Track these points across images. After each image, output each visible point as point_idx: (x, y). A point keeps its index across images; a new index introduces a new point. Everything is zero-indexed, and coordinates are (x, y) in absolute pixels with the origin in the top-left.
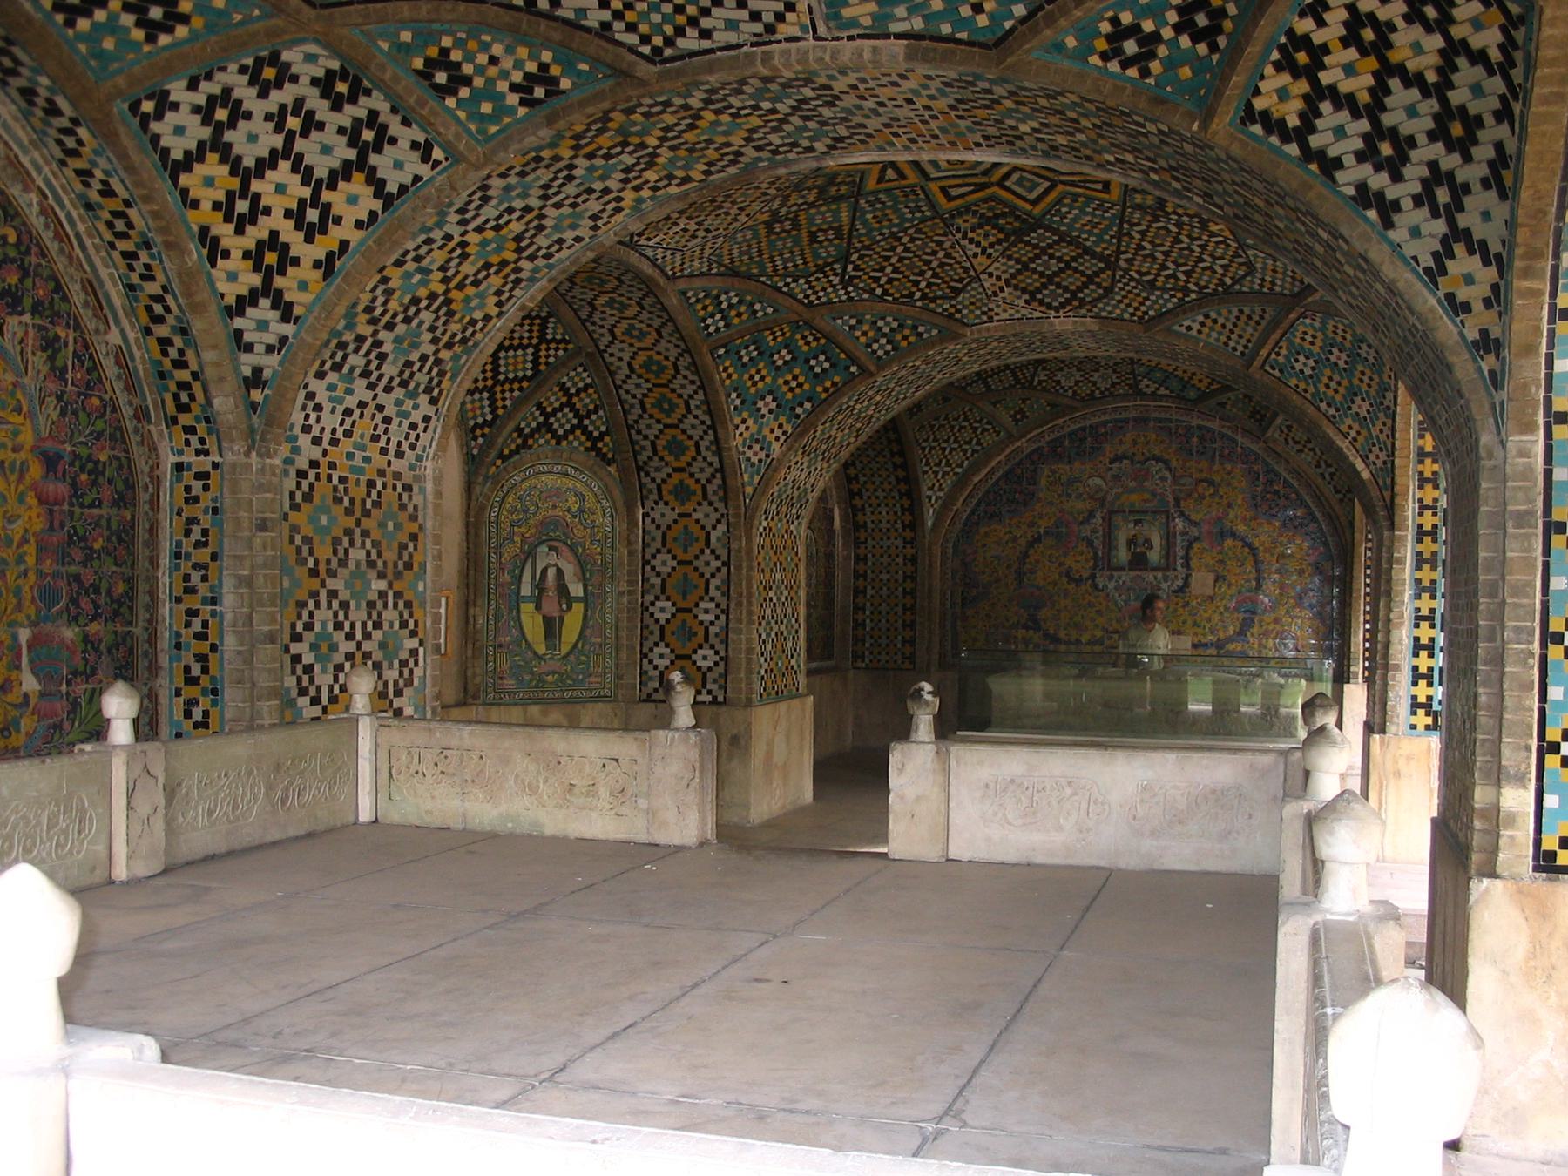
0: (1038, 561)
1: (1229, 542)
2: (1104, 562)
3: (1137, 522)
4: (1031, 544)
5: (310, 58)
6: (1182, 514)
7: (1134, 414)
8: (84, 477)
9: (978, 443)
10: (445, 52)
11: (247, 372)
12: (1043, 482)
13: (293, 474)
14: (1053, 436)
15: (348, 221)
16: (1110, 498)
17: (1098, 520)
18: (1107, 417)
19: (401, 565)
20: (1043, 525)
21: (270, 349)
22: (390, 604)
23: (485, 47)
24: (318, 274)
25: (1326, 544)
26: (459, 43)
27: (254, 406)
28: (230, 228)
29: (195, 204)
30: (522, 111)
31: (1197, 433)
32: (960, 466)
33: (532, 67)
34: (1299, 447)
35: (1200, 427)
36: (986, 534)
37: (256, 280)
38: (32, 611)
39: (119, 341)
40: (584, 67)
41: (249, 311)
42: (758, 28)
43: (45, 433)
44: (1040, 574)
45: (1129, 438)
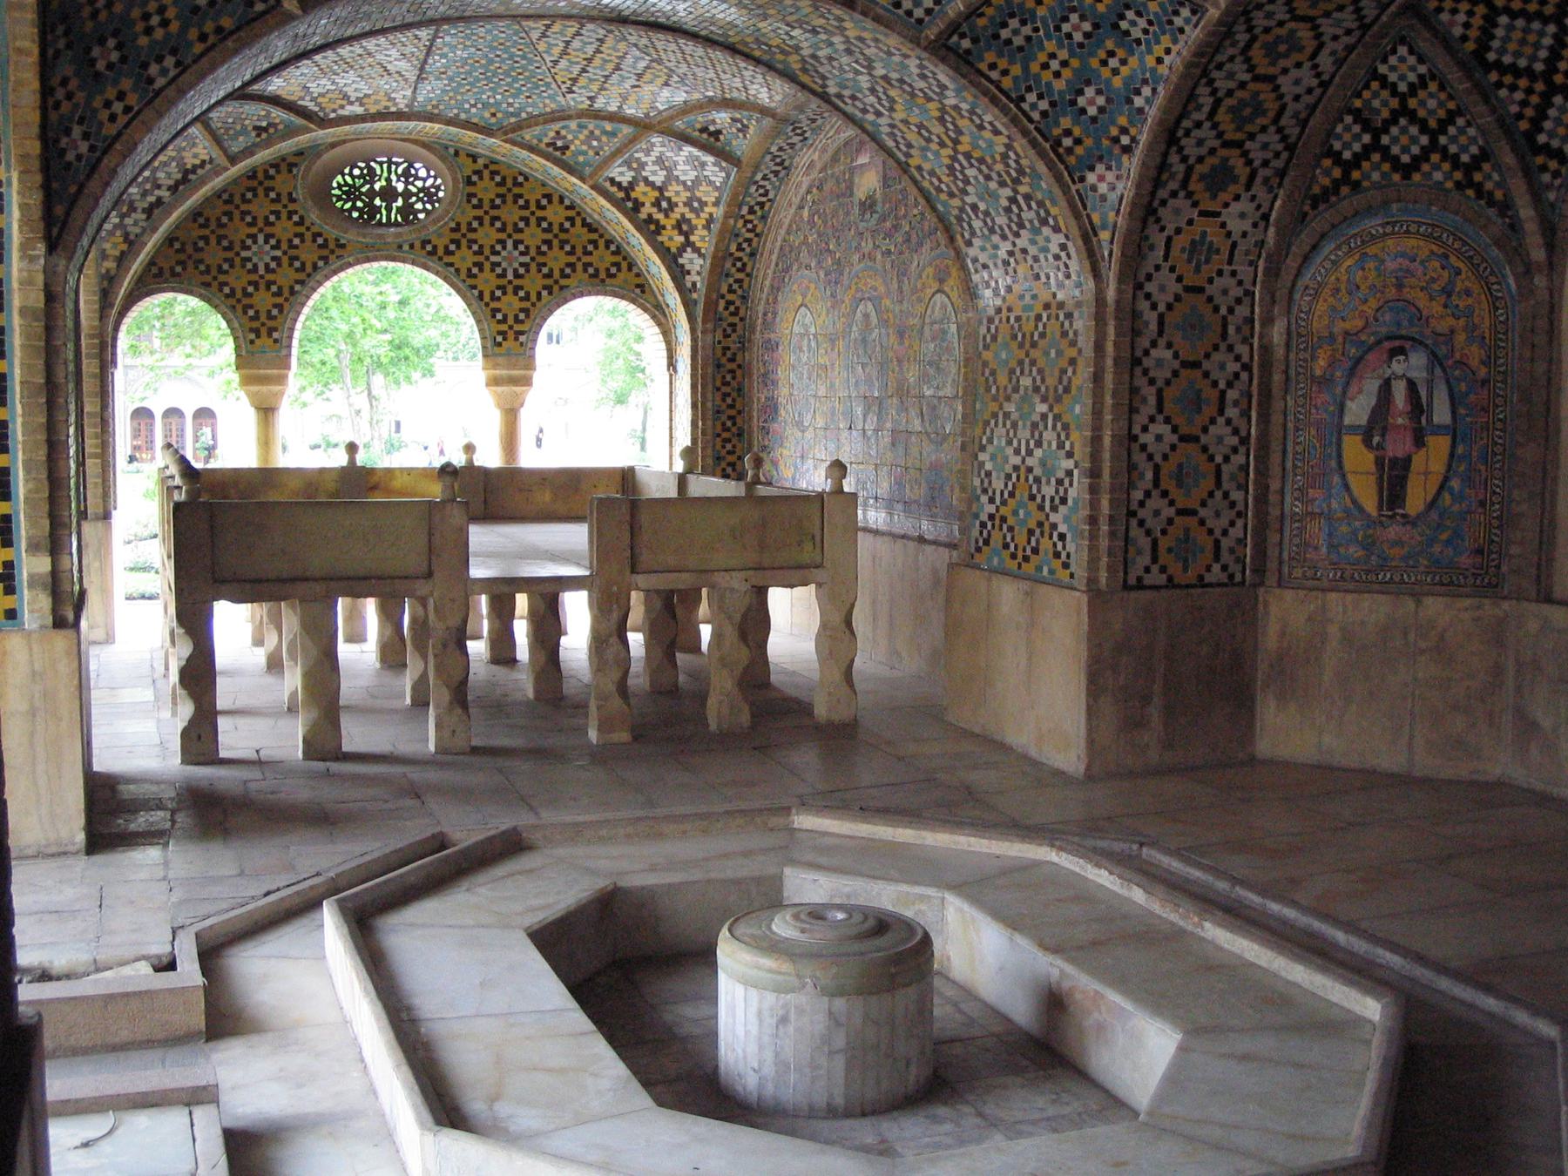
19: (1060, 388)
22: (1050, 425)
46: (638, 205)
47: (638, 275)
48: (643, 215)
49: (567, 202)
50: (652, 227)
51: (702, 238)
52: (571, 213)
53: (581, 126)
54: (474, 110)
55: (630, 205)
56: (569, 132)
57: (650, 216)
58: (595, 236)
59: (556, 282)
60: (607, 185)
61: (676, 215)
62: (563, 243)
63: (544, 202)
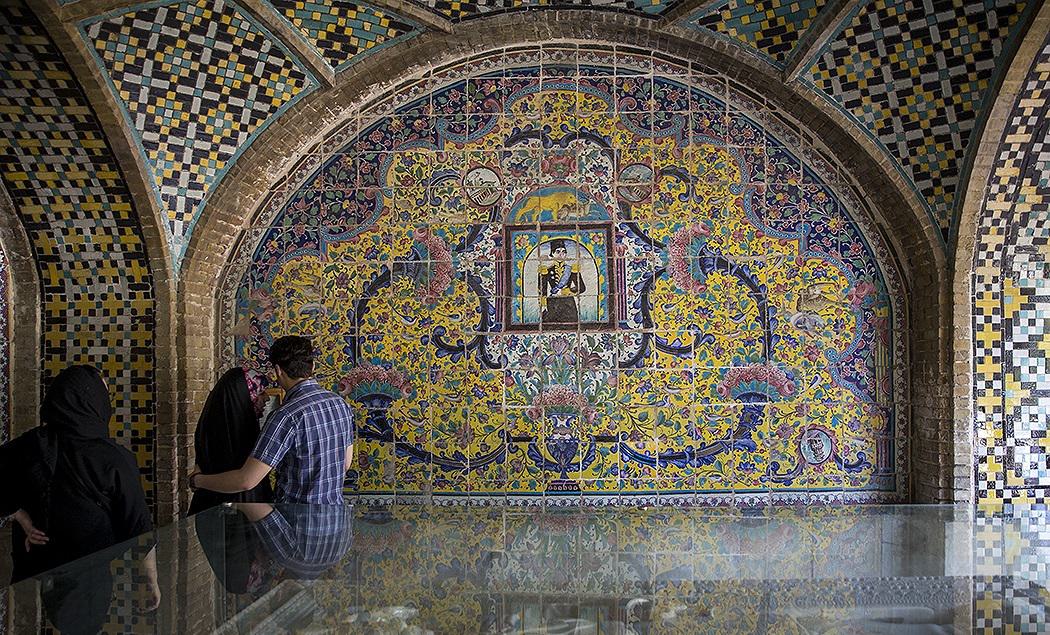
0: (383, 318)
1: (715, 278)
2: (499, 317)
3: (555, 245)
4: (372, 290)
6: (634, 228)
7: (545, 60)
9: (262, 97)
12: (391, 179)
14: (406, 100)
16: (507, 204)
17: (487, 244)
18: (502, 66)
20: (392, 253)
25: (877, 277)
31: (656, 90)
32: (231, 141)
34: (855, 95)
35: (658, 81)
36: (294, 273)
44: (388, 340)
45: (538, 101)
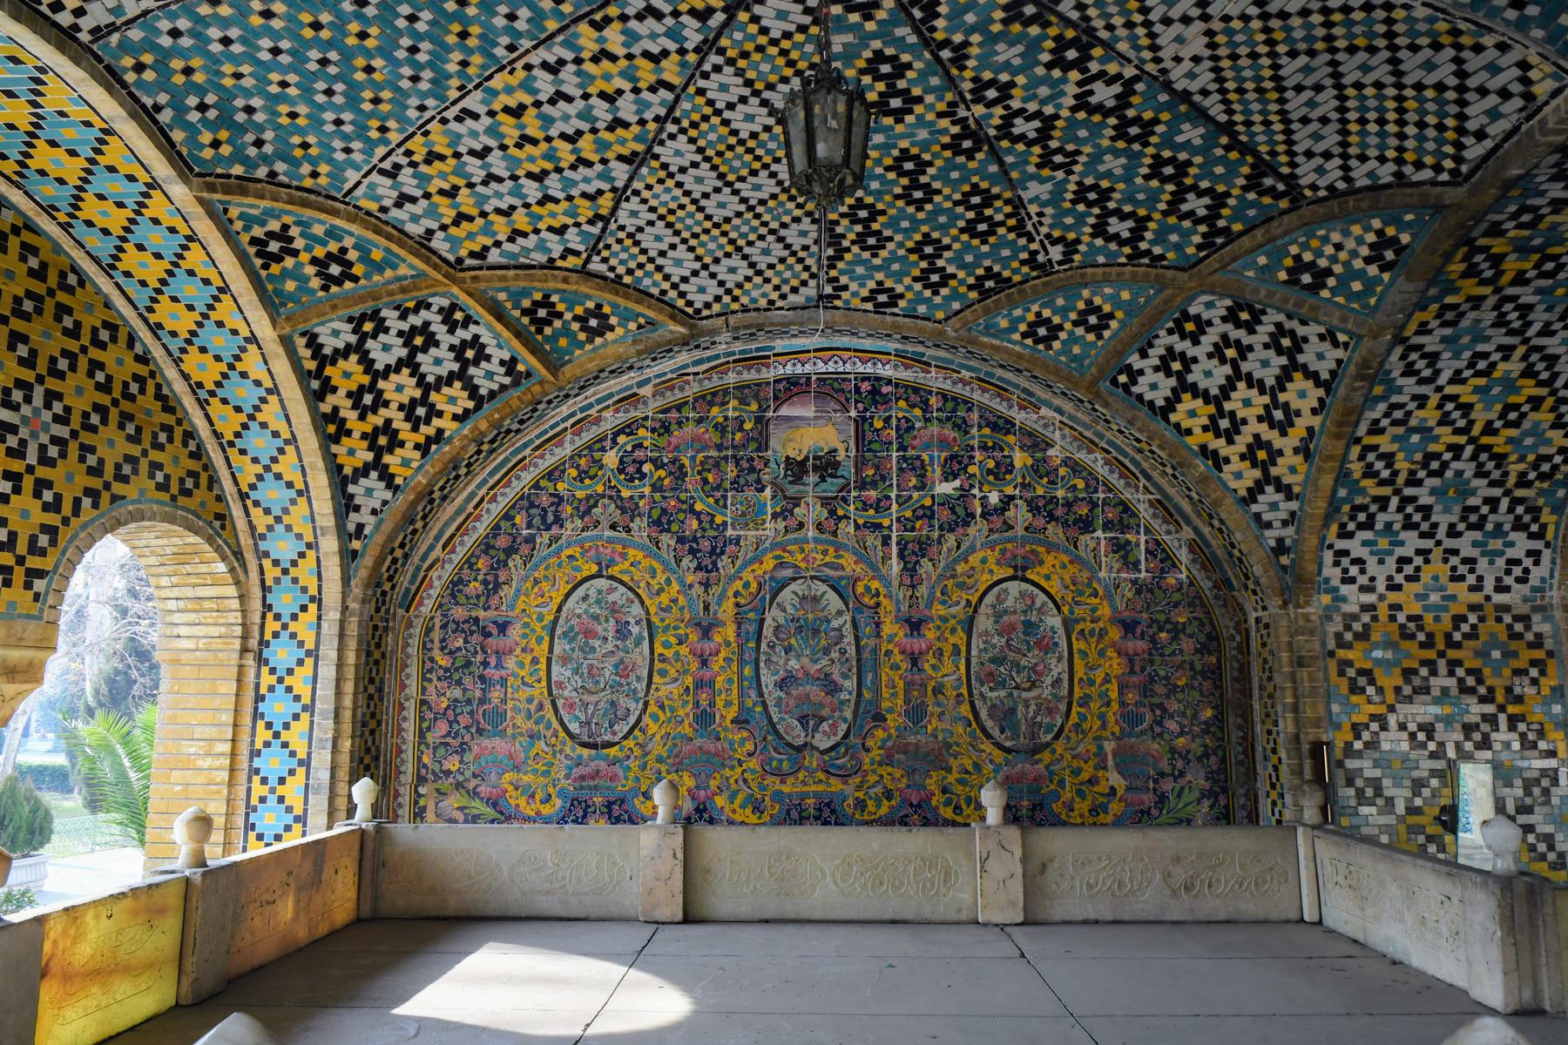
5: (1209, 305)
8: (1163, 635)
10: (1297, 258)
11: (1273, 543)
13: (1338, 618)
15: (1306, 412)
21: (1285, 523)
23: (1325, 240)
24: (1299, 459)
26: (1305, 247)
27: (1284, 568)
28: (1222, 441)
29: (1189, 432)
30: (1386, 276)
33: (1371, 238)
37: (1257, 473)
38: (1117, 730)
39: (1192, 535)
40: (1409, 217)
41: (1260, 498)
42: (1517, 103)
43: (1121, 606)
46: (328, 388)
47: (219, 499)
48: (325, 408)
49: (138, 349)
50: (332, 429)
51: (406, 463)
52: (142, 370)
53: (332, 233)
54: (194, 116)
55: (315, 384)
56: (302, 235)
57: (336, 409)
58: (170, 419)
59: (107, 486)
60: (301, 342)
61: (377, 420)
62: (126, 417)
63: (104, 335)
